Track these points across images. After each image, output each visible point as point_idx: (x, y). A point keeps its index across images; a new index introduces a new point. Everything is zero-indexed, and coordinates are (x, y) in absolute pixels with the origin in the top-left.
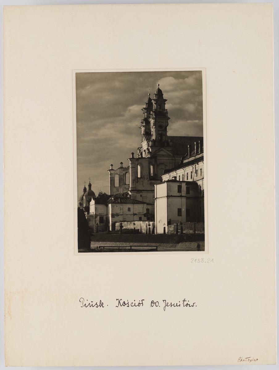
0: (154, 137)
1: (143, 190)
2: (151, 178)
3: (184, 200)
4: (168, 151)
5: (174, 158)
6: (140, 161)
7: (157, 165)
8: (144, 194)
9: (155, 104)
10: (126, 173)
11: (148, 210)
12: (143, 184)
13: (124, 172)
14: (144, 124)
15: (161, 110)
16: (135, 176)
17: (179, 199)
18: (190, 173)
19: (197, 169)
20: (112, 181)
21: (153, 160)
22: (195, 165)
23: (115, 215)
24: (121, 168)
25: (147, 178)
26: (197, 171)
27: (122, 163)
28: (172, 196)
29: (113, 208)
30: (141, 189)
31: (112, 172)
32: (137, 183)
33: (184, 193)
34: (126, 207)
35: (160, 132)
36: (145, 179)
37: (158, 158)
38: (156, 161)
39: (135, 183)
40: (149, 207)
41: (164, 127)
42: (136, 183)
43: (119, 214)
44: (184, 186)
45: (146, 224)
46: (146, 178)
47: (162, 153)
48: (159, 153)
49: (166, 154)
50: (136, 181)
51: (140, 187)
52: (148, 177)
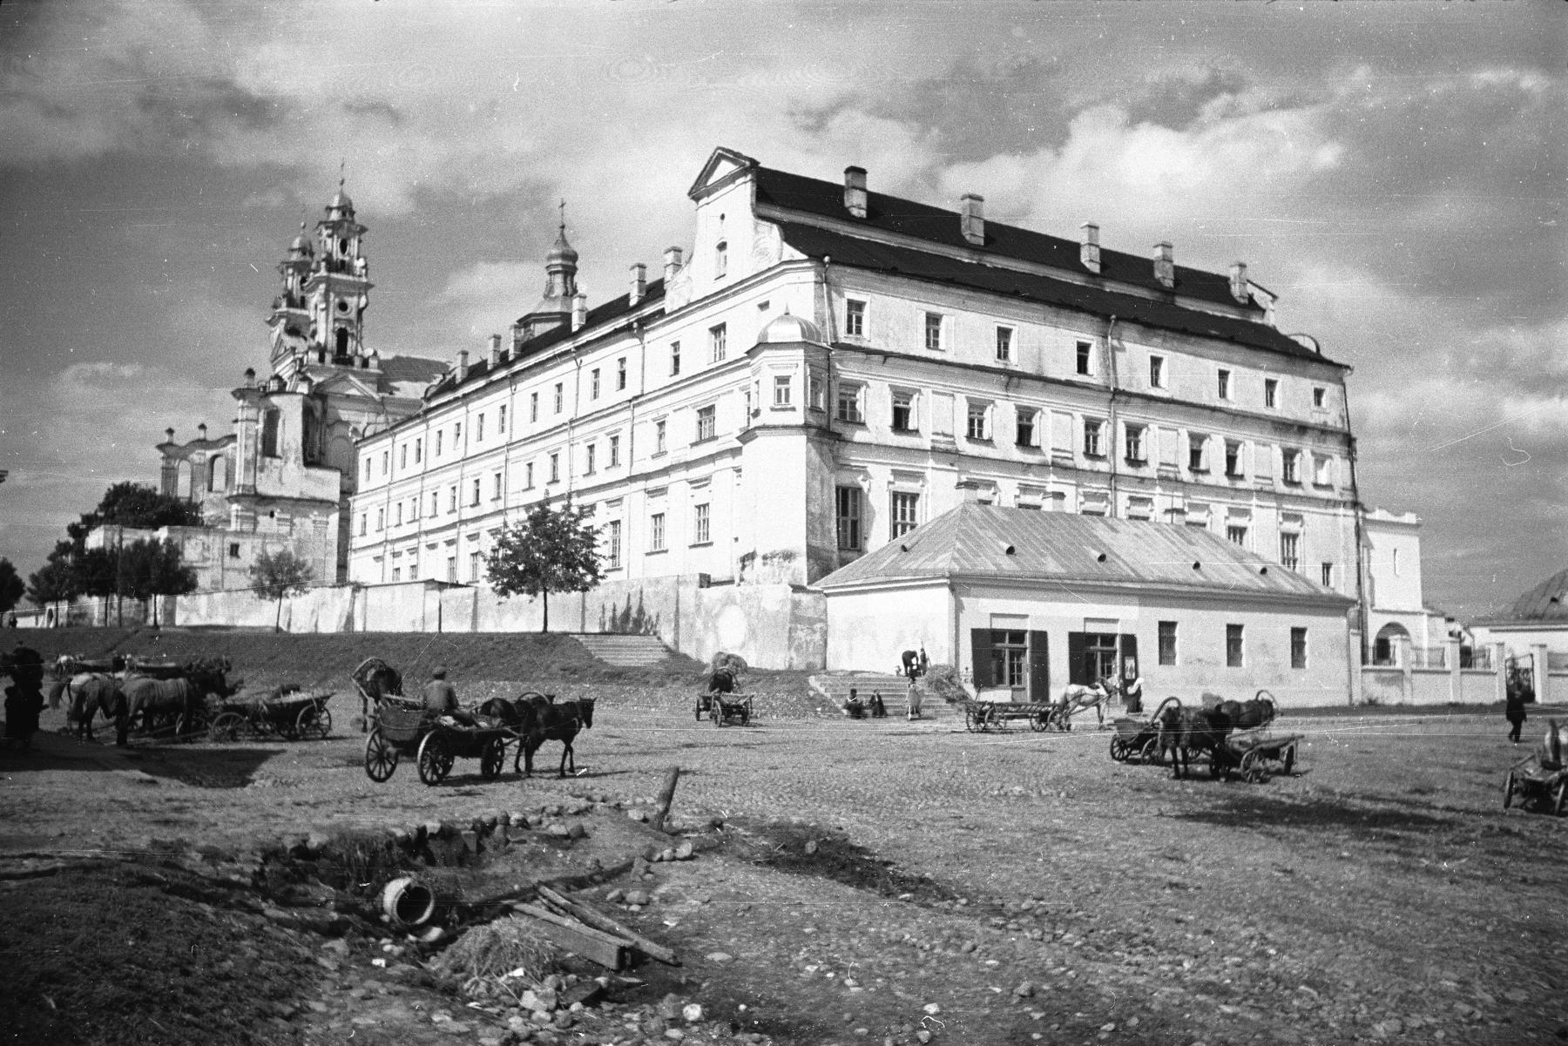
0: (321, 338)
1: (281, 498)
2: (309, 459)
6: (275, 400)
9: (330, 236)
14: (284, 308)
15: (347, 259)
20: (169, 474)
21: (318, 404)
25: (297, 459)
30: (272, 492)
31: (171, 451)
32: (262, 470)
38: (325, 412)
46: (293, 458)
51: (266, 487)
52: (301, 456)
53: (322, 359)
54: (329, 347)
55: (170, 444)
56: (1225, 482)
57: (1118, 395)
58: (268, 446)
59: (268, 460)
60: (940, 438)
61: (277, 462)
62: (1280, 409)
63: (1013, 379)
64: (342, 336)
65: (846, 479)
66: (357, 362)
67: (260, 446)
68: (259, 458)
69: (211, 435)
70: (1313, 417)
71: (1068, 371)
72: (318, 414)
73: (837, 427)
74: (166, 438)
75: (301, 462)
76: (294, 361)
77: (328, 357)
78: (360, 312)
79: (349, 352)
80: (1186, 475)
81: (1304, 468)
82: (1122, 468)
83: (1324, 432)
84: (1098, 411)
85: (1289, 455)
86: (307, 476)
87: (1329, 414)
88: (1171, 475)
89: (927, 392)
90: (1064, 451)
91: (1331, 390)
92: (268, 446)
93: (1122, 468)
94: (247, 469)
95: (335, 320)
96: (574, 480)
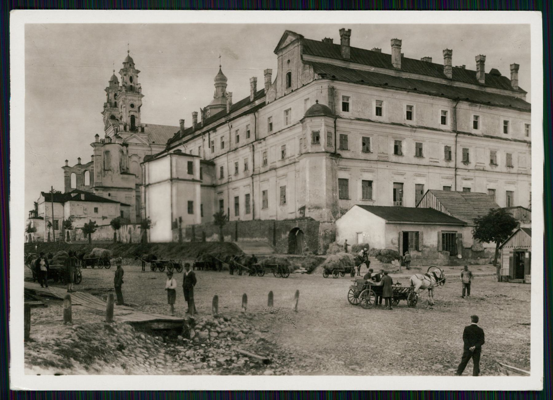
1: (112, 188)
2: (122, 171)
3: (198, 187)
4: (142, 138)
5: (149, 149)
6: (108, 147)
7: (129, 157)
8: (113, 193)
10: (86, 171)
11: (122, 212)
12: (112, 179)
13: (83, 170)
16: (101, 168)
17: (190, 185)
18: (197, 149)
19: (212, 140)
21: (124, 148)
22: (209, 134)
23: (77, 218)
24: (79, 164)
25: (118, 171)
26: (213, 142)
27: (79, 159)
28: (178, 179)
29: (73, 207)
32: (104, 177)
33: (197, 176)
35: (132, 113)
36: (115, 172)
37: (130, 147)
38: (127, 151)
39: (101, 176)
40: (125, 209)
41: (137, 107)
42: (103, 178)
43: (81, 216)
44: (197, 164)
45: (128, 228)
46: (116, 171)
47: (134, 141)
48: (130, 141)
49: (140, 143)
50: (103, 174)
52: (119, 170)
53: (125, 128)
54: (128, 123)
55: (67, 166)
59: (106, 172)
60: (382, 155)
61: (110, 172)
64: (133, 118)
65: (343, 175)
66: (140, 130)
67: (103, 167)
68: (103, 171)
69: (83, 162)
71: (437, 123)
72: (125, 152)
73: (339, 152)
74: (64, 165)
75: (119, 172)
76: (114, 130)
77: (128, 127)
79: (136, 125)
80: (488, 167)
84: (449, 140)
86: (122, 178)
88: (482, 168)
90: (435, 159)
93: (461, 165)
94: (98, 176)
95: (129, 112)
96: (230, 177)
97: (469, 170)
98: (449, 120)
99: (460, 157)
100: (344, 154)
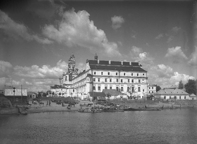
34: (60, 89)
56: (132, 83)
57: (120, 77)
58: (66, 80)
62: (139, 76)
63: (109, 77)
64: (73, 68)
70: (143, 76)
78: (75, 65)
81: (141, 81)
82: (120, 83)
83: (144, 78)
85: (139, 81)
87: (145, 76)
89: (101, 78)
91: (145, 74)
92: (66, 80)
97: (122, 84)
98: (118, 74)
99: (120, 81)
100: (95, 82)
